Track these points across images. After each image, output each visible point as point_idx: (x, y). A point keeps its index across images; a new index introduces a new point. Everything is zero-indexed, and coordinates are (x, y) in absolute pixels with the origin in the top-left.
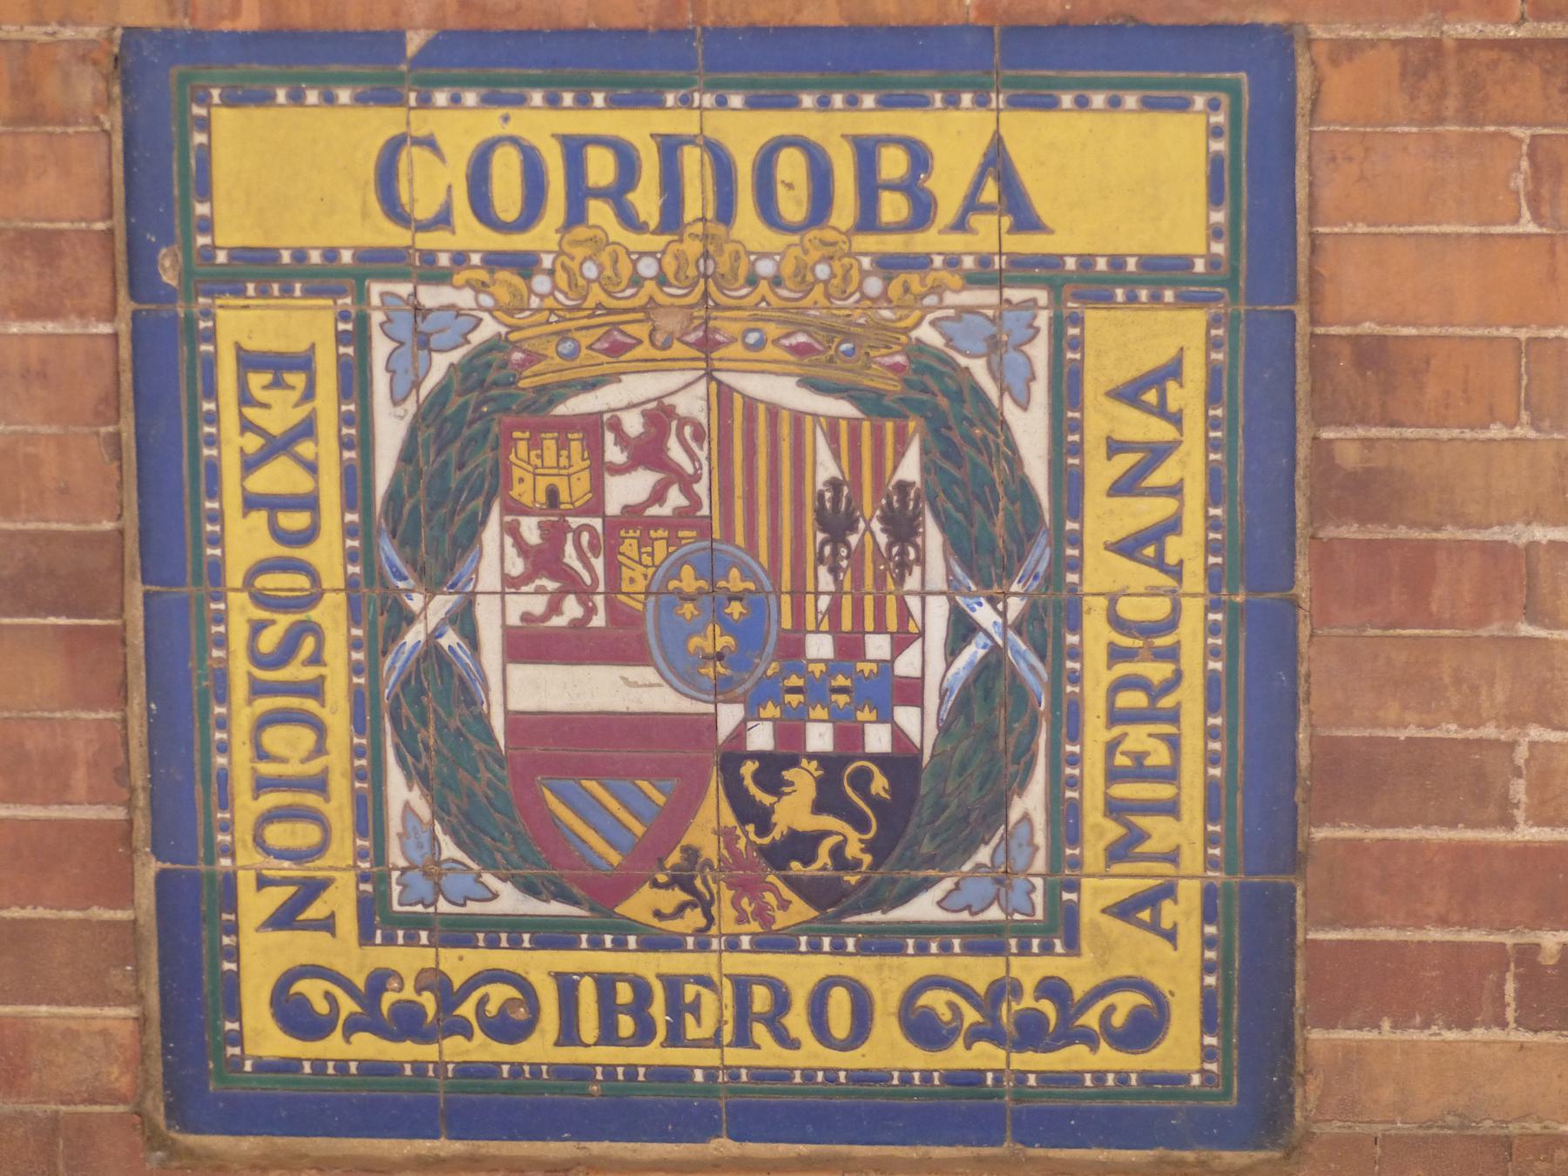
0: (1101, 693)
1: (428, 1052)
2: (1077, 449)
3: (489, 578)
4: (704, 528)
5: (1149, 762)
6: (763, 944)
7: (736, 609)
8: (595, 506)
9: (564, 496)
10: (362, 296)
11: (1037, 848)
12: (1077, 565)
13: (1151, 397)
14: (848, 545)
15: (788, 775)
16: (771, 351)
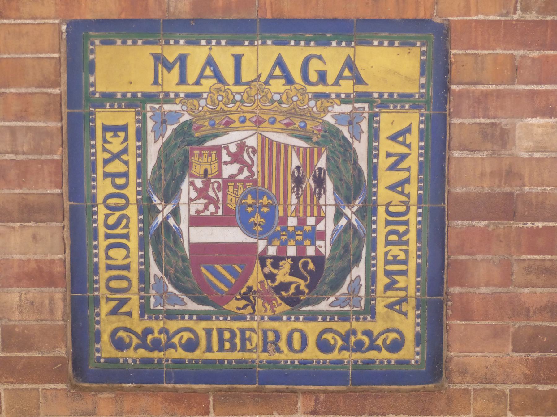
0: (384, 234)
1: (161, 355)
2: (377, 156)
3: (184, 198)
4: (255, 182)
5: (398, 258)
6: (271, 319)
7: (265, 210)
8: (220, 175)
9: (209, 172)
10: (144, 108)
11: (361, 285)
12: (375, 194)
13: (401, 139)
14: (302, 188)
15: (281, 263)
16: (278, 125)
